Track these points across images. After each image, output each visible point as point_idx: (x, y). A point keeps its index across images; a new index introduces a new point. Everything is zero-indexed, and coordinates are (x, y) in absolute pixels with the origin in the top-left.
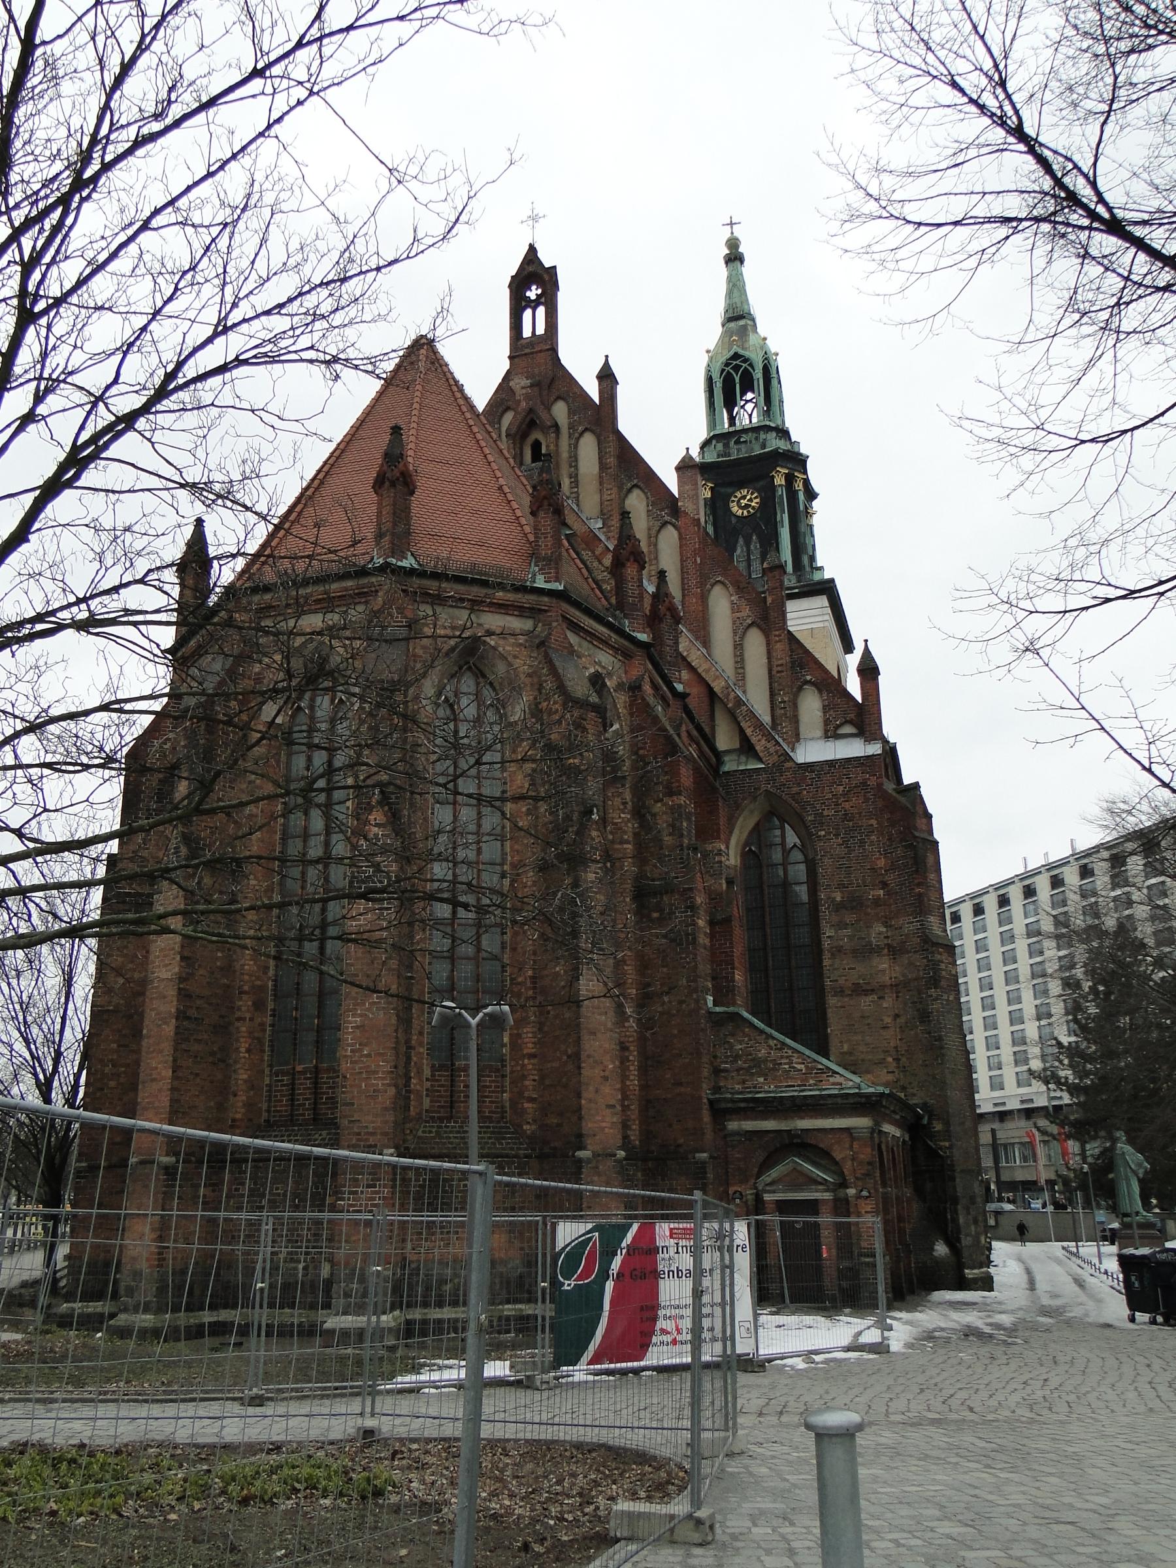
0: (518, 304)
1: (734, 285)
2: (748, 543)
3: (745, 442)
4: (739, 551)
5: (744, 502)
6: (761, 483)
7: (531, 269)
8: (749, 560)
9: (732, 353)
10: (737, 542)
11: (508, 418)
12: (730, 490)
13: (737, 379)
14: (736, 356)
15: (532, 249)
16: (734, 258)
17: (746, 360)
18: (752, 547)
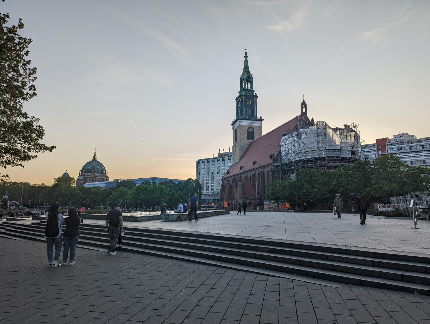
0: (302, 107)
1: (246, 62)
2: (249, 109)
3: (249, 92)
4: (247, 110)
5: (249, 102)
6: (251, 100)
7: (304, 103)
8: (249, 112)
9: (248, 75)
10: (247, 109)
11: (302, 122)
12: (247, 99)
13: (248, 80)
14: (248, 76)
15: (304, 101)
16: (246, 57)
17: (250, 77)
18: (249, 110)
